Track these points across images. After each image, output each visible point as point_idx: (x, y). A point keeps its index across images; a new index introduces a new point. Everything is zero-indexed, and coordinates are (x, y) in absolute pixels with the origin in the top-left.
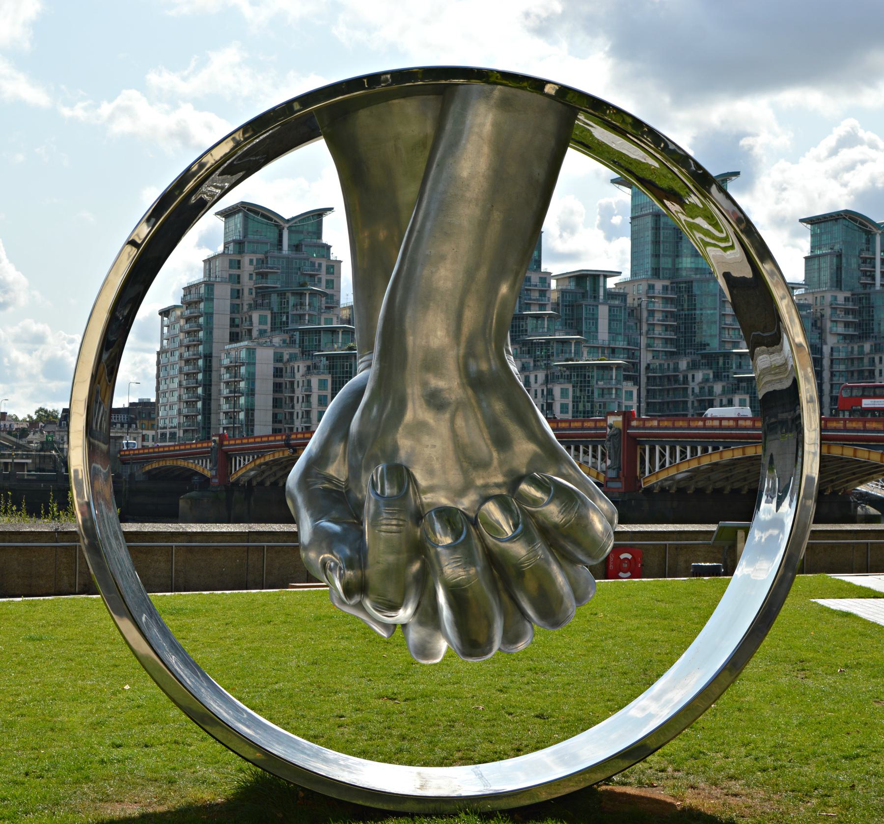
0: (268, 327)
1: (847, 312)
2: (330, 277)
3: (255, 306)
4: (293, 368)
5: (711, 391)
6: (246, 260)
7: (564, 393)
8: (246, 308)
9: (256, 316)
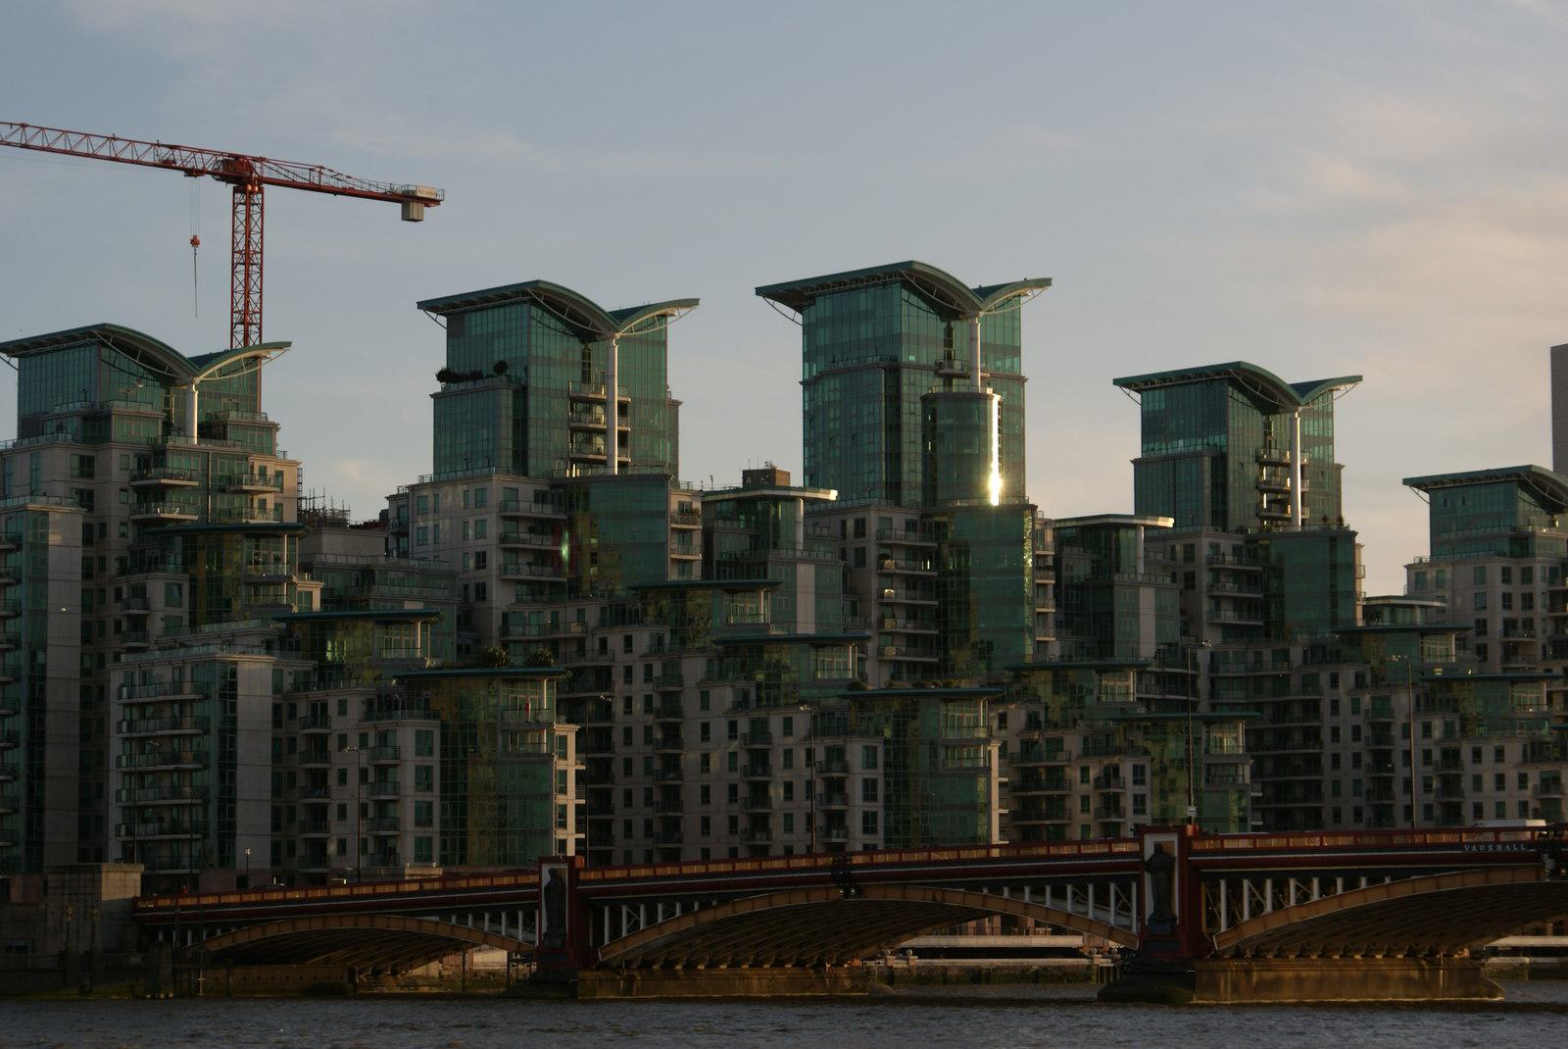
0: (184, 612)
3: (140, 561)
4: (320, 712)
9: (156, 589)
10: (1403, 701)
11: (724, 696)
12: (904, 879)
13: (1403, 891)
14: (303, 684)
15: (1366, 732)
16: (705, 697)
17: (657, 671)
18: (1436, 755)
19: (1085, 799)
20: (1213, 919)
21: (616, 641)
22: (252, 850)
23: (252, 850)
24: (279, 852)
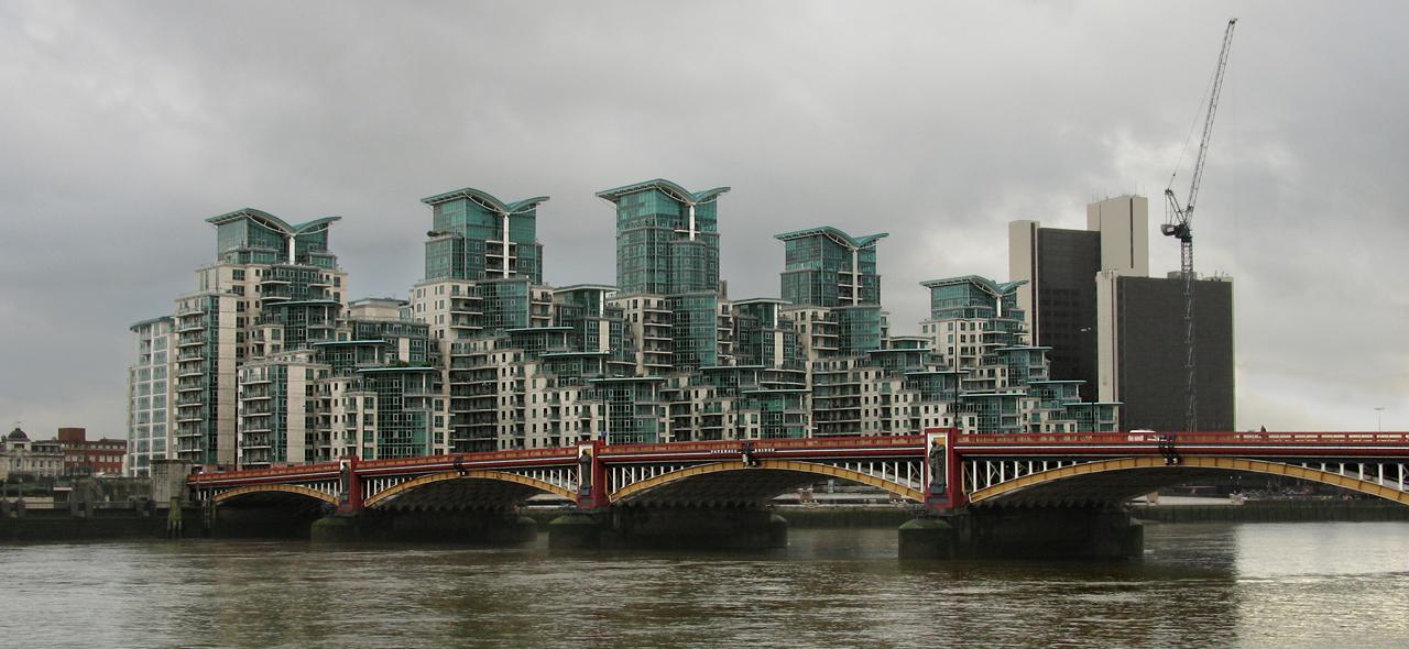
0: (281, 342)
1: (827, 328)
2: (338, 290)
3: (262, 320)
4: (327, 388)
5: (718, 407)
6: (251, 272)
7: (602, 410)
8: (252, 321)
10: (895, 386)
11: (541, 383)
12: (485, 468)
13: (688, 473)
14: (323, 374)
15: (879, 399)
16: (534, 381)
17: (515, 371)
18: (909, 410)
19: (731, 430)
20: (610, 489)
21: (499, 357)
22: (296, 452)
23: (296, 452)
24: (310, 455)
